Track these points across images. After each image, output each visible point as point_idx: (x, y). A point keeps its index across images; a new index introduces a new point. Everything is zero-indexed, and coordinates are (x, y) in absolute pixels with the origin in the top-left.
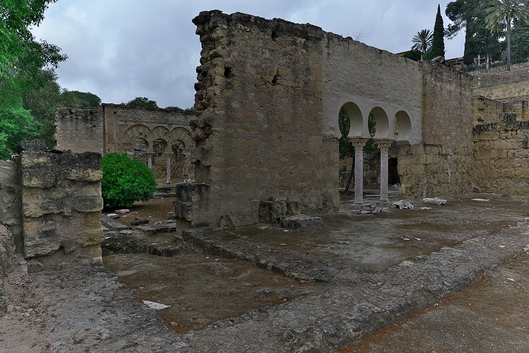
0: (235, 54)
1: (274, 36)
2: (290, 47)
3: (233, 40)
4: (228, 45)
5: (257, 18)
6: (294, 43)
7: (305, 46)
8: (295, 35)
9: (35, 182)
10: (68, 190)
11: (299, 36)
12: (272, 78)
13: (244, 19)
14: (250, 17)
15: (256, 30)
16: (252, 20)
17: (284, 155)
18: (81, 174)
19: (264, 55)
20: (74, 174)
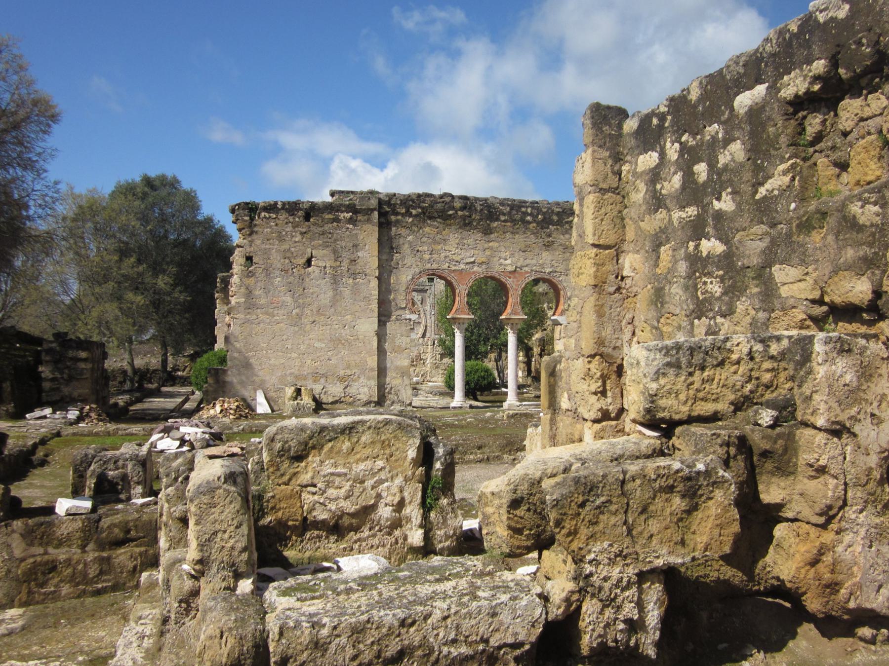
0: (258, 242)
1: (307, 217)
2: (330, 225)
3: (256, 229)
4: (250, 235)
5: (284, 204)
6: (337, 220)
7: (351, 221)
8: (337, 211)
9: (48, 358)
10: (68, 364)
11: (342, 212)
12: (303, 260)
13: (271, 208)
14: (276, 203)
15: (283, 216)
16: (279, 206)
17: (320, 340)
18: (74, 354)
19: (294, 239)
20: (71, 354)
